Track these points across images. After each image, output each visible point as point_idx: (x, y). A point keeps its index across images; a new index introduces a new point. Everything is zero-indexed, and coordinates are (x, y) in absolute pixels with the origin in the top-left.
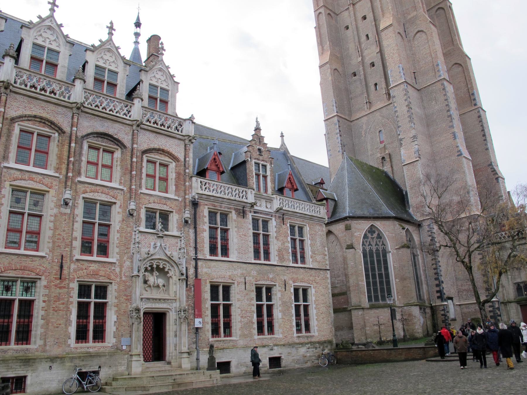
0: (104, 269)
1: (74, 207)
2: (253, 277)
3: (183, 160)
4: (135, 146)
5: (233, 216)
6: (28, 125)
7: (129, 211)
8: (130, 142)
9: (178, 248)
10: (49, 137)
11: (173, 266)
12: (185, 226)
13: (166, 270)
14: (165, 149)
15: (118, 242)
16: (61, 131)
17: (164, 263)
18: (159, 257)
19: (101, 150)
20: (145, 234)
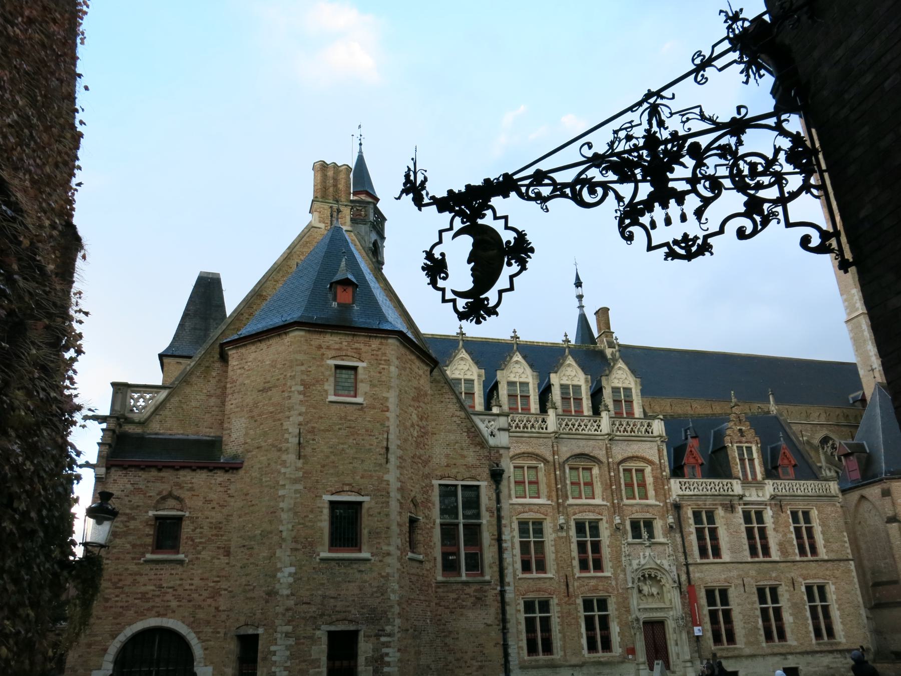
1: (568, 529)
2: (752, 577)
3: (658, 462)
4: (610, 460)
5: (720, 513)
8: (605, 457)
10: (536, 468)
11: (664, 574)
13: (658, 578)
14: (639, 455)
16: (545, 461)
19: (581, 469)
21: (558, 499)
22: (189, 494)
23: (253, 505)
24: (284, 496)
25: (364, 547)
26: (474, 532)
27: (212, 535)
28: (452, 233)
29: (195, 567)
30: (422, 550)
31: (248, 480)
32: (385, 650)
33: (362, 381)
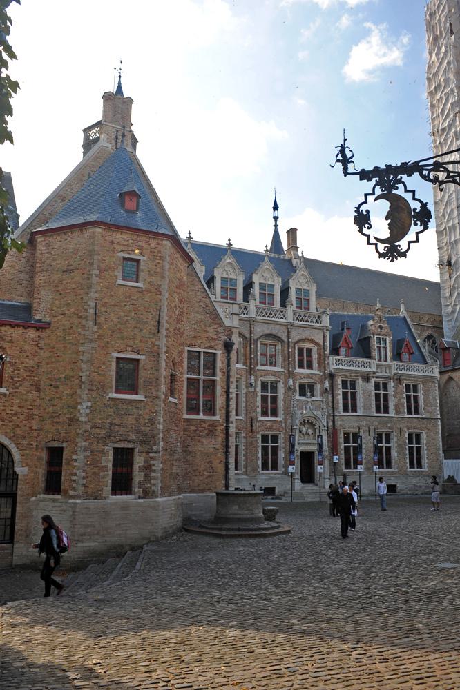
1: (256, 386)
4: (290, 340)
12: (325, 393)
22: (10, 344)
23: (58, 356)
24: (83, 351)
25: (141, 391)
26: (211, 385)
27: (27, 376)
28: (374, 197)
29: (14, 398)
30: (177, 396)
31: (54, 338)
32: (152, 462)
33: (142, 271)
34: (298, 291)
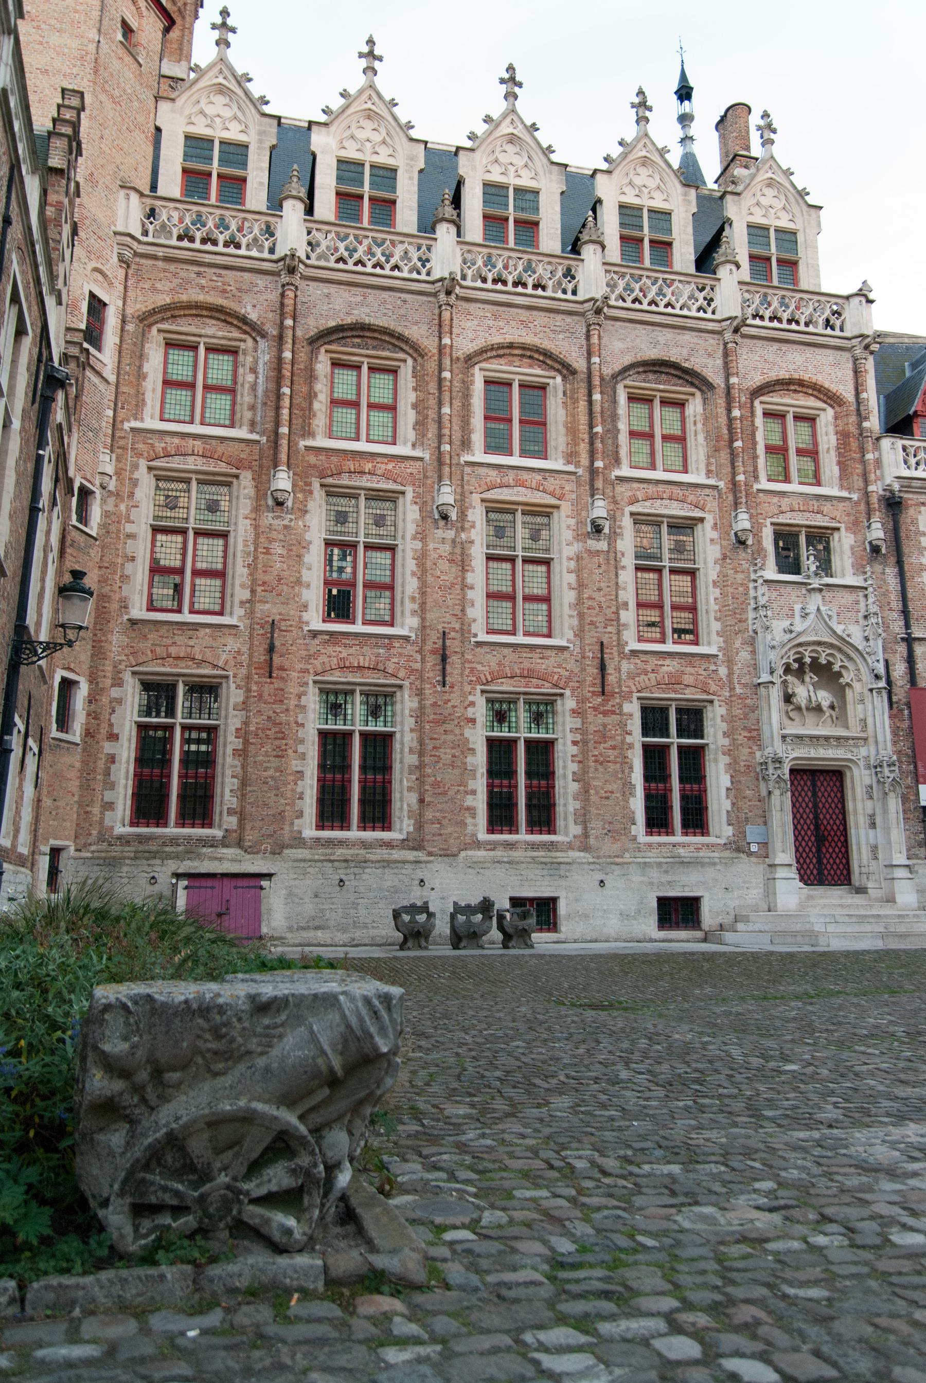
0: (692, 670)
1: (614, 535)
4: (734, 380)
6: (500, 368)
7: (736, 534)
9: (861, 615)
10: (543, 388)
11: (850, 659)
12: (871, 561)
13: (836, 668)
15: (717, 608)
16: (567, 370)
17: (828, 651)
18: (815, 639)
19: (657, 402)
20: (778, 586)
21: (592, 462)
34: (757, 231)
